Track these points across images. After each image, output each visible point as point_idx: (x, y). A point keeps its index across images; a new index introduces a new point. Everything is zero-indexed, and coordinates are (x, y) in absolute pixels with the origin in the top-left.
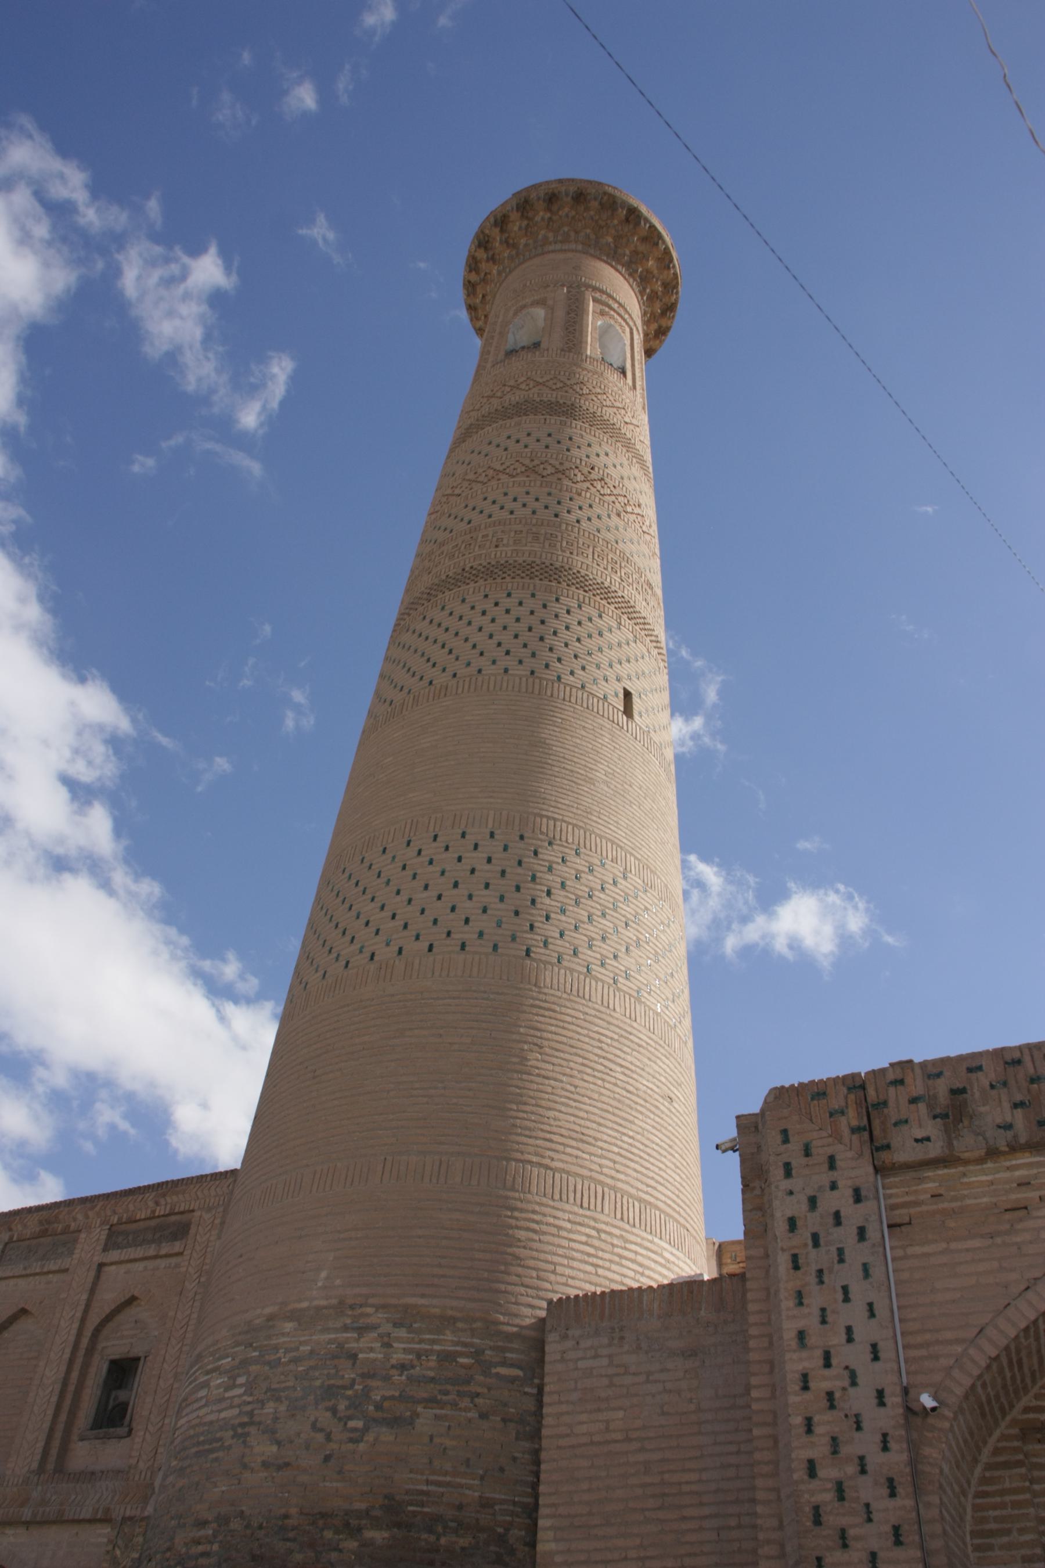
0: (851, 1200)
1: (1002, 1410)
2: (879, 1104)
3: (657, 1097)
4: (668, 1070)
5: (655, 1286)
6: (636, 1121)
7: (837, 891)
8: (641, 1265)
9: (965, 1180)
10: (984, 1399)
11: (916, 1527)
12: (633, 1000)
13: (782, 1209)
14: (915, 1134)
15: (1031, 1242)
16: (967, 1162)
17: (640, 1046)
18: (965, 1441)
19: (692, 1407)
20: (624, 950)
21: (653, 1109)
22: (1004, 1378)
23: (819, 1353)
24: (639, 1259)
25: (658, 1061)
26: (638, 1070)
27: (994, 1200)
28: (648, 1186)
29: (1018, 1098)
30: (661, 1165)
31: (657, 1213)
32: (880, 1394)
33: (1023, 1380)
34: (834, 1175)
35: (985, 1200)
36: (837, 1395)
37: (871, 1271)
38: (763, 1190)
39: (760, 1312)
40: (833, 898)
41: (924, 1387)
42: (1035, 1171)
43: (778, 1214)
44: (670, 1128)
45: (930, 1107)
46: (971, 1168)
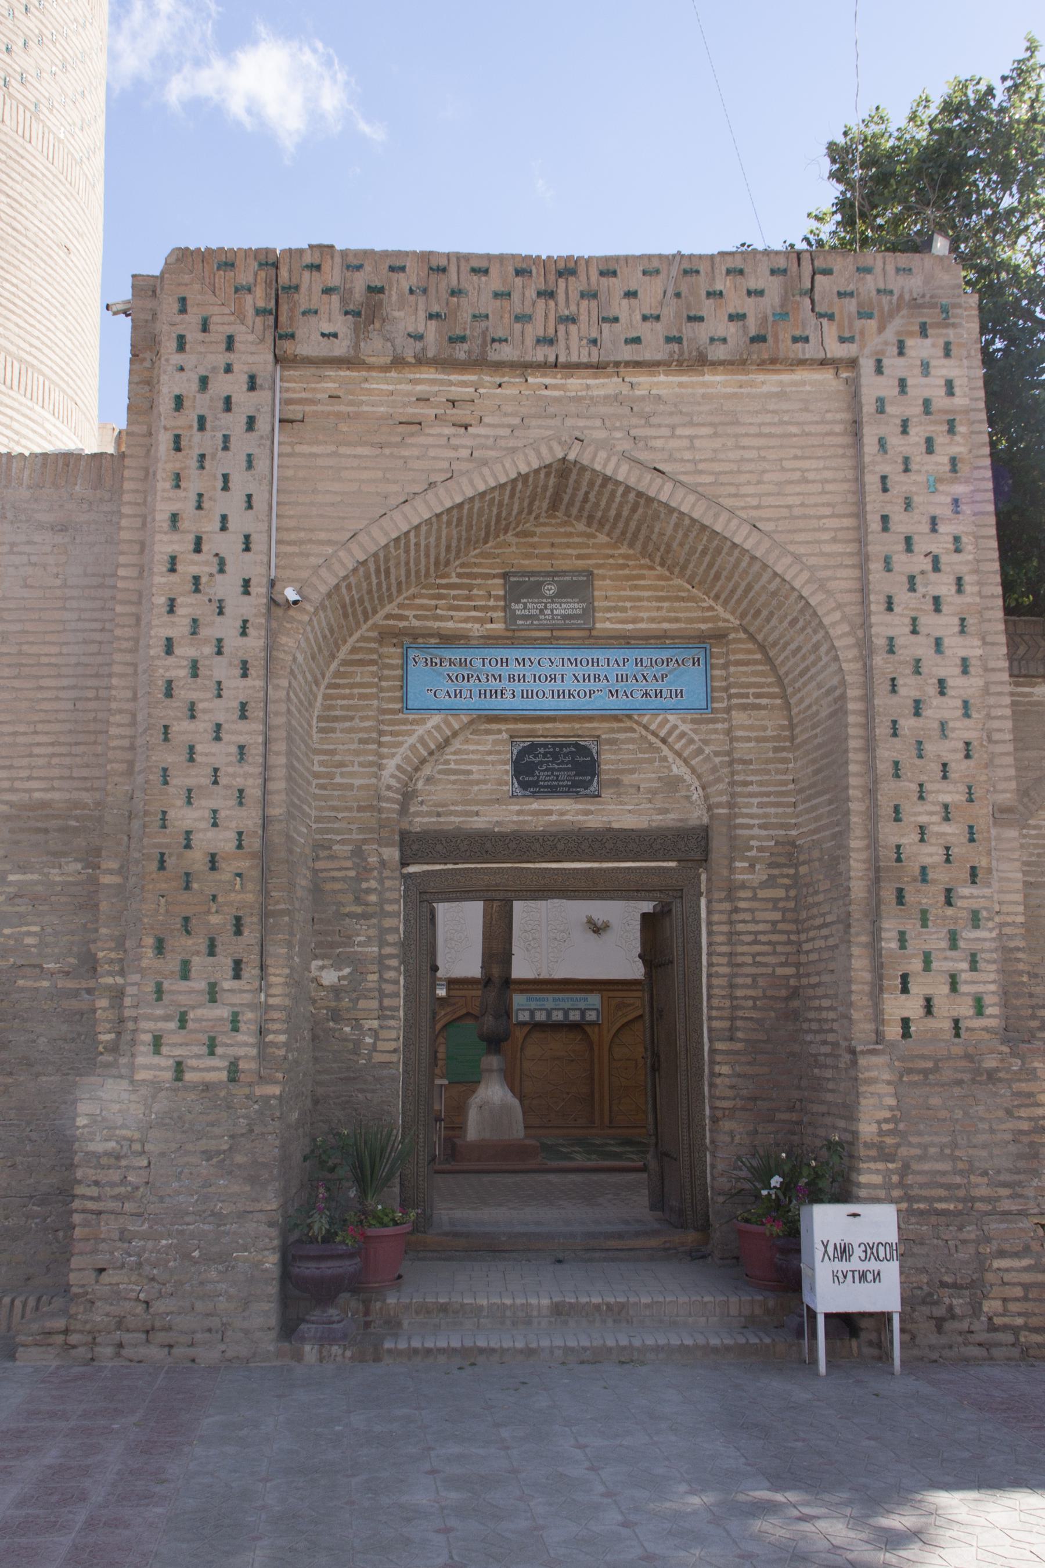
0: (245, 387)
1: (365, 612)
2: (290, 288)
3: (49, 242)
4: (67, 214)
5: (27, 454)
6: (22, 267)
7: (315, 51)
8: (17, 433)
9: (366, 386)
10: (347, 599)
11: (262, 705)
12: (28, 114)
13: (170, 384)
14: (324, 328)
15: (418, 458)
16: (370, 368)
17: (33, 175)
18: (324, 637)
19: (58, 582)
20: (21, 44)
21: (45, 257)
22: (370, 584)
23: (191, 538)
24: (15, 425)
25: (56, 200)
26: (29, 206)
27: (391, 411)
28: (31, 345)
29: (436, 309)
30: (49, 325)
31: (41, 379)
32: (247, 583)
33: (389, 589)
34: (231, 357)
35: (382, 409)
36: (204, 580)
37: (254, 463)
38: (153, 363)
39: (137, 491)
40: (307, 57)
41: (290, 581)
42: (436, 388)
43: (165, 390)
44: (64, 284)
45: (343, 301)
46: (374, 374)
